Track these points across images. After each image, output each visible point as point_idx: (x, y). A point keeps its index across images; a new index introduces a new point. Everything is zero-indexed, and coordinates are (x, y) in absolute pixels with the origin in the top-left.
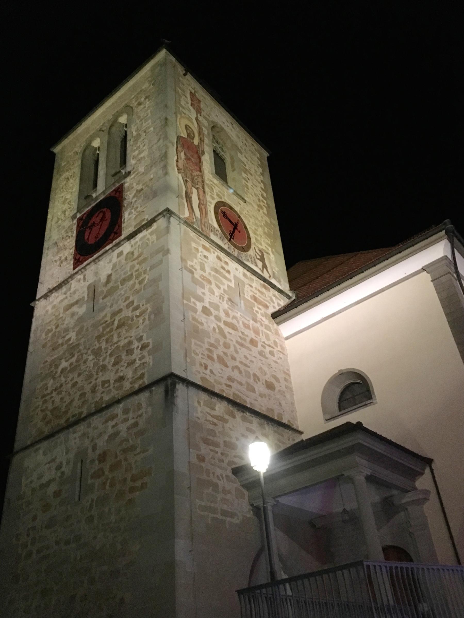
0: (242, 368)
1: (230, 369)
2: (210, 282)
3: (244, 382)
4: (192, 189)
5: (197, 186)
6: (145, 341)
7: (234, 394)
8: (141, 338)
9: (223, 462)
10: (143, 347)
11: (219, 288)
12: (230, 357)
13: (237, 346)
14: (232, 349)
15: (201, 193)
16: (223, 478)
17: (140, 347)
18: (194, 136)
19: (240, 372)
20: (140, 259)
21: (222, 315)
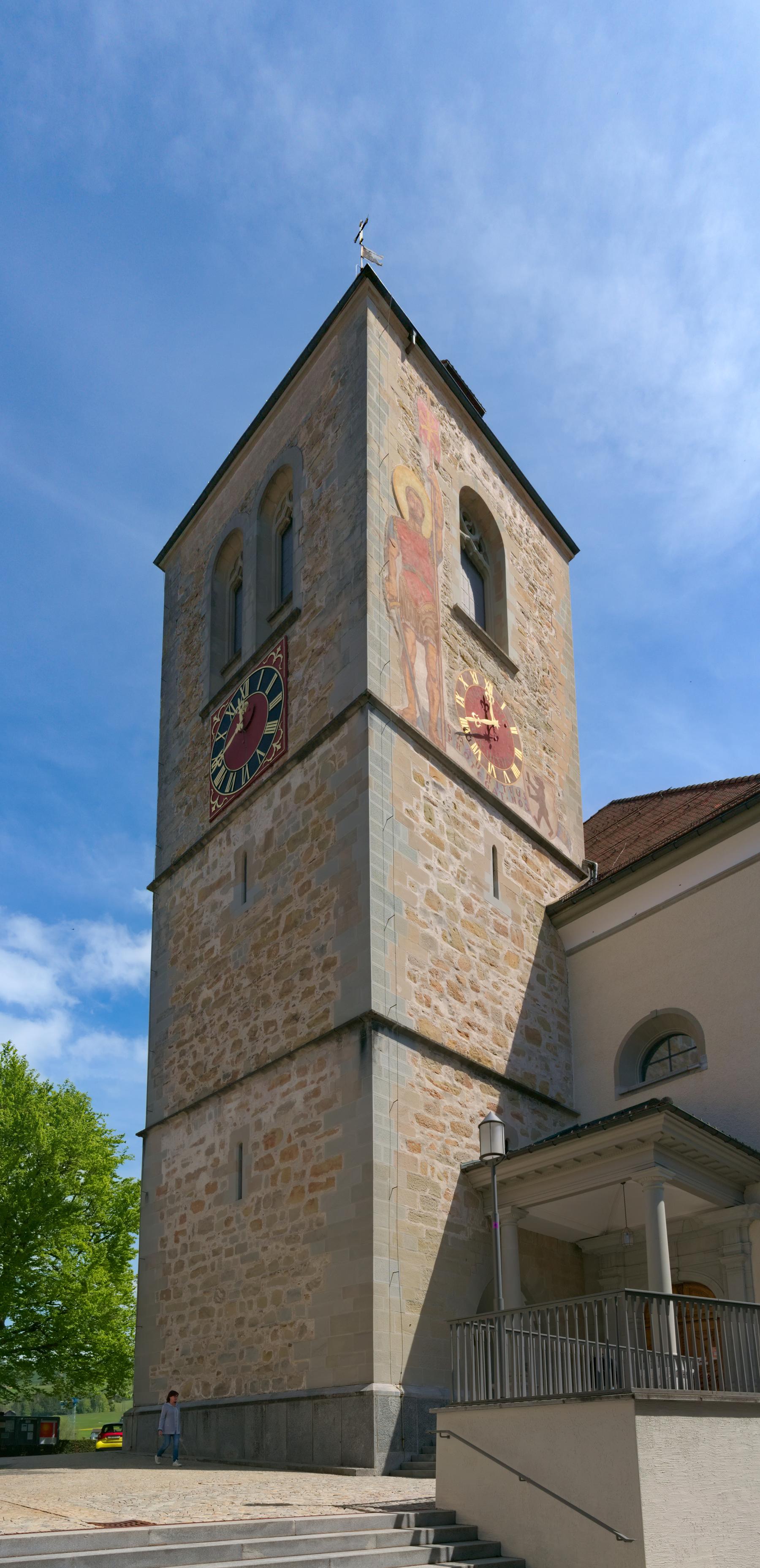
0: (489, 1005)
1: (467, 1006)
2: (440, 845)
3: (490, 1029)
4: (414, 644)
5: (425, 638)
6: (329, 955)
7: (473, 1048)
8: (322, 950)
9: (447, 1153)
10: (327, 966)
11: (458, 857)
12: (468, 985)
13: (484, 966)
14: (474, 972)
15: (433, 654)
16: (447, 1177)
17: (322, 965)
18: (424, 515)
19: (485, 1012)
20: (320, 799)
21: (461, 908)
